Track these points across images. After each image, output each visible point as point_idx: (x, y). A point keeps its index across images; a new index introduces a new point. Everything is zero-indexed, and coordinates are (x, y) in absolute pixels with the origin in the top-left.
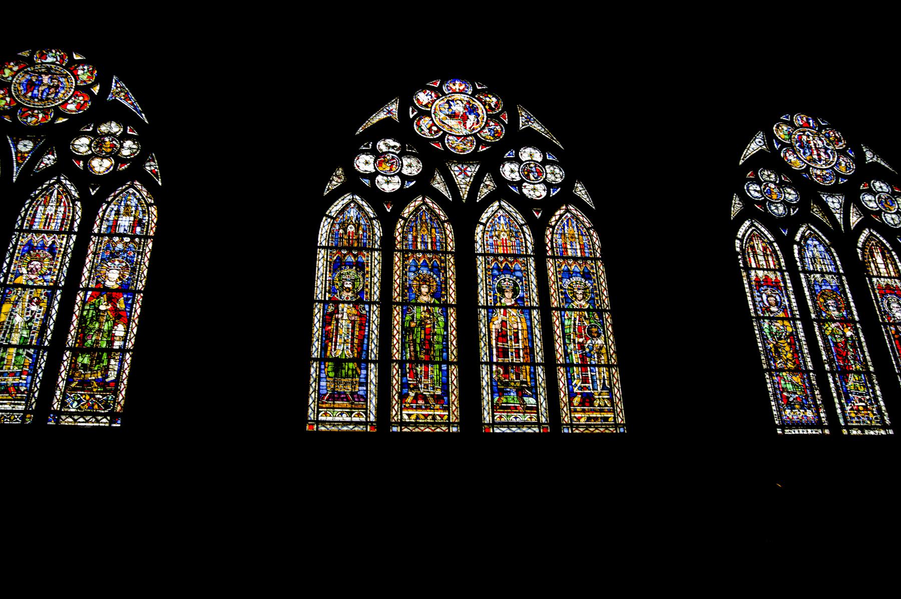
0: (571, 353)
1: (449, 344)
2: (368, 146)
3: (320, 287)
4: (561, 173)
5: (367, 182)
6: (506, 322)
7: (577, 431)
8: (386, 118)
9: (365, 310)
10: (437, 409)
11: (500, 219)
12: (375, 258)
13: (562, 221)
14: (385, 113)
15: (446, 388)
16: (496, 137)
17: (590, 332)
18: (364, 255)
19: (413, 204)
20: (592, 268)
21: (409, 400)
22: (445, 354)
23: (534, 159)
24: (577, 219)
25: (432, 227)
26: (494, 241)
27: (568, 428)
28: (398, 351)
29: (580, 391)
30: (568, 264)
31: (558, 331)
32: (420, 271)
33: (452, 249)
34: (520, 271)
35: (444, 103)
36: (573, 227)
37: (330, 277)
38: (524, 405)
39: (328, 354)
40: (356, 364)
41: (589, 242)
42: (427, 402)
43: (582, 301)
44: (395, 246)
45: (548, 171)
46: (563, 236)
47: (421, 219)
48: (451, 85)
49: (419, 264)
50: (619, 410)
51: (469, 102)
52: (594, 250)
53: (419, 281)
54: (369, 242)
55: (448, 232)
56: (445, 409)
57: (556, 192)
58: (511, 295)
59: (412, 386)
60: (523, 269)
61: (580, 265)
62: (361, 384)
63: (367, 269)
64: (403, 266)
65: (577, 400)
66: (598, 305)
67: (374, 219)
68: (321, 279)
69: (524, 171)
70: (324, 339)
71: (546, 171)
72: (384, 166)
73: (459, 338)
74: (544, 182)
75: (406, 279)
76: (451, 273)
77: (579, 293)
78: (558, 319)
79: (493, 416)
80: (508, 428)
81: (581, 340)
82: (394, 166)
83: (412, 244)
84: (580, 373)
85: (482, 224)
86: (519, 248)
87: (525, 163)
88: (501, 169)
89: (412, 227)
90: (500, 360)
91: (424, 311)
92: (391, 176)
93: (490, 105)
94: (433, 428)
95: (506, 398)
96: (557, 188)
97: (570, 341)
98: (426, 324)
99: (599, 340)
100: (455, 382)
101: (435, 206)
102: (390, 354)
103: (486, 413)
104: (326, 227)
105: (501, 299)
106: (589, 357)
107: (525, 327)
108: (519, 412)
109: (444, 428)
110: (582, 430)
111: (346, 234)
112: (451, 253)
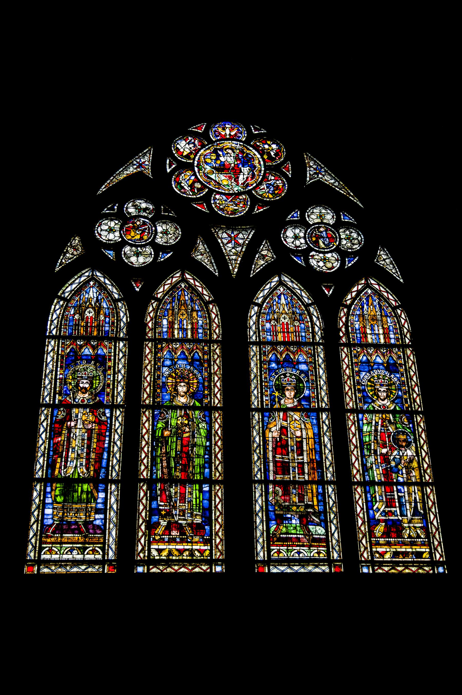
0: (372, 468)
1: (213, 457)
2: (112, 208)
3: (49, 387)
4: (360, 238)
5: (111, 254)
6: (286, 428)
7: (380, 571)
8: (136, 173)
10: (196, 542)
12: (121, 350)
13: (360, 299)
14: (135, 167)
15: (208, 514)
16: (276, 194)
17: (396, 440)
18: (105, 347)
19: (169, 282)
20: (399, 357)
21: (159, 531)
22: (207, 470)
24: (380, 296)
25: (193, 310)
26: (272, 326)
27: (368, 567)
28: (146, 467)
29: (384, 518)
30: (368, 353)
31: (354, 438)
33: (218, 337)
34: (305, 363)
35: (210, 153)
37: (60, 374)
38: (309, 536)
39: (57, 472)
40: (92, 485)
41: (395, 325)
43: (386, 401)
44: (146, 334)
45: (343, 236)
47: (179, 300)
50: (436, 543)
51: (242, 152)
52: (401, 335)
53: (175, 378)
54: (113, 330)
55: (213, 316)
56: (206, 542)
58: (293, 393)
59: (163, 513)
60: (309, 360)
61: (383, 354)
62: (98, 511)
63: (110, 364)
64: (155, 359)
65: (380, 529)
66: (407, 405)
67: (119, 300)
68: (50, 377)
69: (311, 237)
70: (51, 453)
71: (340, 235)
72: (133, 234)
73: (225, 450)
74: (338, 250)
75: (159, 377)
77: (382, 390)
78: (354, 423)
79: (269, 551)
80: (289, 566)
81: (384, 451)
82: (146, 233)
83: (167, 332)
84: (383, 493)
88: (282, 236)
89: (167, 310)
91: (181, 416)
92: (141, 246)
93: (269, 154)
94: (190, 568)
96: (355, 258)
97: (370, 452)
98: (184, 432)
99: (408, 451)
100: (219, 507)
101: (197, 284)
102: (136, 471)
103: (259, 548)
104: (58, 312)
105: (280, 400)
106: (395, 473)
107: (311, 434)
108: (303, 546)
109: (204, 568)
110: (386, 569)
111: (83, 320)
112: (216, 341)
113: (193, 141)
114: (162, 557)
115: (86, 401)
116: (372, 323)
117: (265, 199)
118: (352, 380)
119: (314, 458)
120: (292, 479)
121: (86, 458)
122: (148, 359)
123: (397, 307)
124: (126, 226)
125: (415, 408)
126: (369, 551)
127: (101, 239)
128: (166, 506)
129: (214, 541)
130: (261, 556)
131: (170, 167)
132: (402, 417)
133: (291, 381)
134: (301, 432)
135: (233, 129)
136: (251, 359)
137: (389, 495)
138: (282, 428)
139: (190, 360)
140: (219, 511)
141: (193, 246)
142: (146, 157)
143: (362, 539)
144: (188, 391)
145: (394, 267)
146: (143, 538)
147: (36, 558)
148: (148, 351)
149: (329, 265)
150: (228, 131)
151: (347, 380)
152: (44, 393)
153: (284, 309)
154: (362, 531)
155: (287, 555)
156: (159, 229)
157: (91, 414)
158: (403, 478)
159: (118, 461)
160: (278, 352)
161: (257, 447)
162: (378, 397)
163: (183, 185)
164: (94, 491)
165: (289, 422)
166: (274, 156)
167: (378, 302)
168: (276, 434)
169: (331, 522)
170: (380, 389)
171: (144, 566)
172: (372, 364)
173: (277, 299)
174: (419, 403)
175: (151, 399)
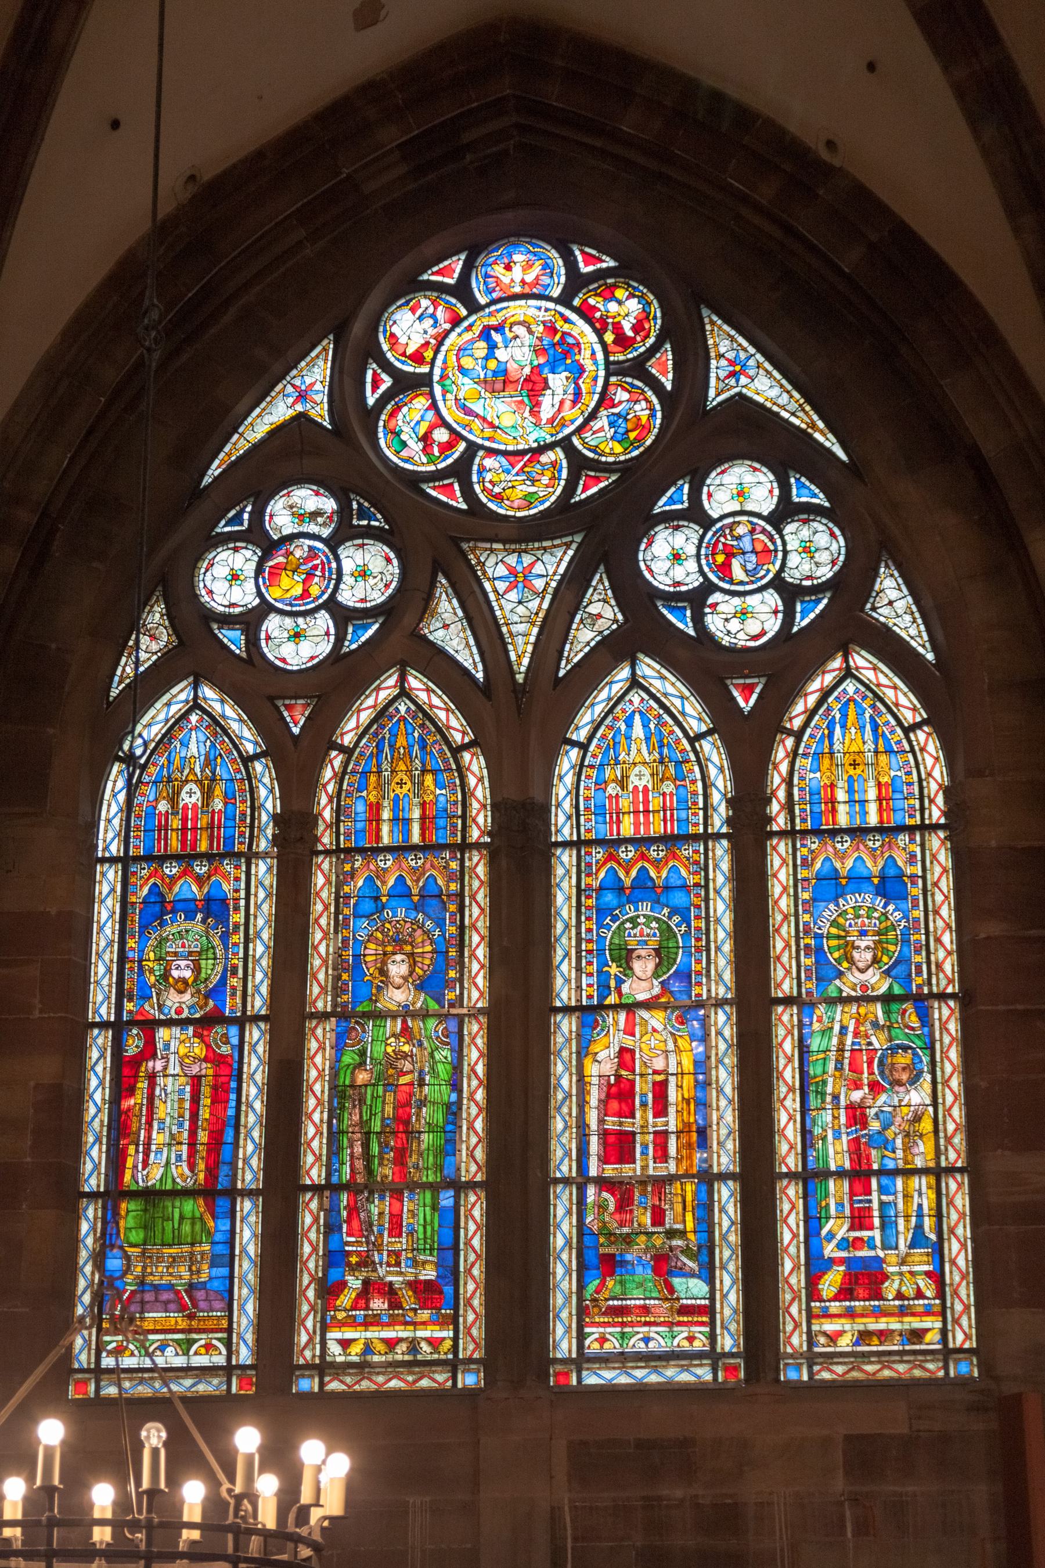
0: (824, 1139)
2: (237, 519)
3: (105, 982)
4: (834, 547)
6: (632, 1052)
7: (826, 1375)
9: (227, 1042)
10: (424, 1323)
11: (629, 725)
13: (829, 709)
14: (290, 400)
18: (226, 877)
19: (370, 702)
20: (912, 859)
21: (345, 1299)
23: (749, 507)
25: (424, 771)
28: (318, 1158)
30: (836, 852)
31: (789, 1068)
32: (388, 913)
35: (472, 341)
36: (862, 728)
39: (128, 1176)
40: (201, 1202)
41: (909, 773)
42: (395, 1304)
44: (318, 840)
45: (793, 544)
46: (826, 762)
47: (392, 746)
48: (499, 270)
49: (384, 890)
50: (959, 1307)
51: (552, 330)
53: (382, 944)
54: (242, 834)
55: (472, 781)
56: (442, 1323)
57: (812, 616)
58: (651, 966)
59: (354, 1259)
60: (692, 880)
63: (239, 918)
64: (337, 900)
65: (831, 1282)
66: (919, 981)
67: (256, 757)
68: (107, 957)
69: (714, 554)
72: (285, 581)
73: (493, 1110)
74: (778, 584)
76: (478, 914)
78: (789, 1032)
79: (581, 1337)
81: (857, 1096)
82: (316, 579)
83: (364, 831)
84: (846, 1198)
85: (574, 744)
86: (683, 815)
87: (719, 525)
88: (641, 557)
90: (610, 1170)
91: (393, 1035)
93: (618, 328)
94: (410, 1378)
95: (622, 1283)
97: (823, 1101)
99: (913, 1093)
100: (476, 1242)
101: (436, 701)
103: (560, 1330)
105: (620, 982)
107: (688, 1065)
109: (440, 1378)
110: (840, 1369)
112: (477, 846)
113: (431, 310)
114: (349, 1358)
115: (186, 1011)
116: (852, 772)
117: (603, 459)
118: (793, 924)
119: (692, 1120)
120: (638, 1173)
121: (189, 1144)
122: (323, 902)
123: (915, 727)
124: (271, 563)
125: (938, 984)
126: (805, 1329)
127: (212, 603)
128: (358, 1243)
129: (461, 1319)
130: (564, 1345)
131: (374, 391)
132: (905, 1011)
133: (648, 935)
134: (667, 1058)
135: (531, 266)
136: (558, 885)
137: (860, 1201)
138: (623, 1051)
139: (416, 898)
140: (475, 1252)
141: (426, 606)
142: (316, 370)
143: (790, 1304)
144: (411, 973)
145: (914, 621)
146: (311, 1317)
147: (92, 1366)
148: (320, 880)
149: (754, 628)
150: (517, 273)
151: (781, 925)
152: (95, 995)
153: (639, 750)
154: (790, 1286)
155: (621, 1346)
156: (348, 566)
157: (196, 1040)
158: (895, 1159)
159: (257, 1146)
160: (620, 864)
161: (565, 1099)
162: (851, 961)
163: (404, 437)
164: (208, 1217)
165: (638, 1035)
166: (630, 334)
167: (871, 716)
168: (609, 1066)
169: (723, 1267)
170: (857, 943)
171: (312, 1377)
172: (844, 882)
173: (623, 727)
174: (949, 973)
175: (329, 998)
